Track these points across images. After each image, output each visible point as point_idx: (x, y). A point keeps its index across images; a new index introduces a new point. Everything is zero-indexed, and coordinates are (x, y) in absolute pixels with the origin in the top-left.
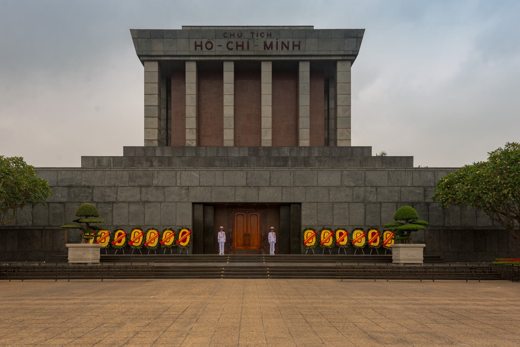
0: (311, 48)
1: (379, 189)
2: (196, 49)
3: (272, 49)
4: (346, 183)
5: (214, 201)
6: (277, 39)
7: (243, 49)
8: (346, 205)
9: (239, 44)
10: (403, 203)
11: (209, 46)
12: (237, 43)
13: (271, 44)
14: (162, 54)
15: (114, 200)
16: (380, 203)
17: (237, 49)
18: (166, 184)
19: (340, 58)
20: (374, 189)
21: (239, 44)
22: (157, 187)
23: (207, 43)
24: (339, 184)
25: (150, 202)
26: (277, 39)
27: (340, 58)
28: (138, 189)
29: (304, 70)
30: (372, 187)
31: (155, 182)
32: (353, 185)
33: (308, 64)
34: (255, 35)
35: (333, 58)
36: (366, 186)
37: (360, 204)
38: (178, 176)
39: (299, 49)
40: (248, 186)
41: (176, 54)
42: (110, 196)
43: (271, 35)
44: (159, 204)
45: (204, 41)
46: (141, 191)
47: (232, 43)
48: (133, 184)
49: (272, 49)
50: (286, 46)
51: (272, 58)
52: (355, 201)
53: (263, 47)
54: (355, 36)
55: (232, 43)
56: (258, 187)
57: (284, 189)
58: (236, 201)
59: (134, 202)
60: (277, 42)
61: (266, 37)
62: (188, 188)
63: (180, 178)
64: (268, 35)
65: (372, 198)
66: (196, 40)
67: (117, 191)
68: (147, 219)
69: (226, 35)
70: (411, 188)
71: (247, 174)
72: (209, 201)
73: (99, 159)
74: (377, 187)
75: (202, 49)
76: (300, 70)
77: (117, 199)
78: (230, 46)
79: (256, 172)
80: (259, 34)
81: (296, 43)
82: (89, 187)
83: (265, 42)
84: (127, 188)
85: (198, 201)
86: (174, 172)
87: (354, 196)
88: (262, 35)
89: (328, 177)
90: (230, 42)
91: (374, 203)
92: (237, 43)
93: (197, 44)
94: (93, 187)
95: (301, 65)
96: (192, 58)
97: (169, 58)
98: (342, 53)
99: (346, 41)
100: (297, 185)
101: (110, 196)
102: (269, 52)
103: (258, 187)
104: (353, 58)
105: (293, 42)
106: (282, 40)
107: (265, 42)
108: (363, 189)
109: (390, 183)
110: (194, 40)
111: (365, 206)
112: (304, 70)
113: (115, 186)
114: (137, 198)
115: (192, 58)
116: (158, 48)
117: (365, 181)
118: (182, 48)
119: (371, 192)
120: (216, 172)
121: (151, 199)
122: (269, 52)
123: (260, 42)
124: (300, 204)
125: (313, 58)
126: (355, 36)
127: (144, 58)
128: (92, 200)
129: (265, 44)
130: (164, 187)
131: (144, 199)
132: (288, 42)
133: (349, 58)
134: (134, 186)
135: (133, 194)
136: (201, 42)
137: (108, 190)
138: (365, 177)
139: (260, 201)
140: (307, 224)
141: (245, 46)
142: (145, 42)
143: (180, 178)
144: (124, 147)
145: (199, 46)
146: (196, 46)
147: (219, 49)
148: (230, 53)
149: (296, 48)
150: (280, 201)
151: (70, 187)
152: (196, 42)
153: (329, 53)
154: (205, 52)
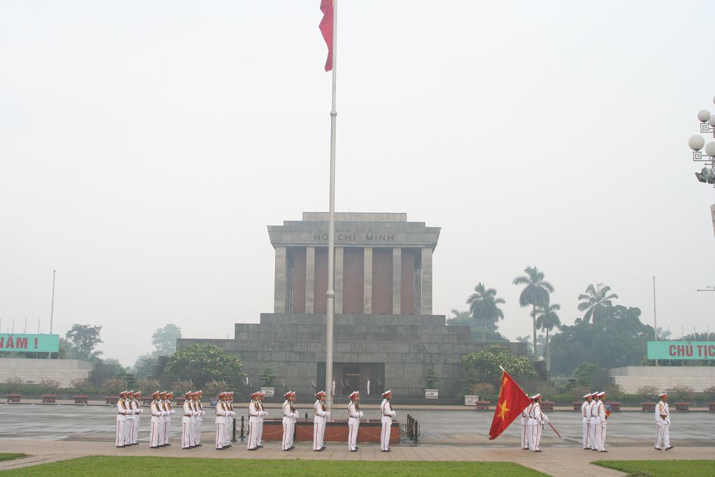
0: (402, 239)
4: (412, 351)
13: (372, 237)
22: (296, 352)
28: (284, 353)
30: (428, 353)
31: (295, 349)
33: (400, 250)
35: (418, 247)
54: (436, 232)
56: (358, 354)
65: (428, 361)
73: (248, 325)
74: (431, 353)
82: (255, 352)
98: (425, 243)
102: (370, 242)
110: (313, 234)
112: (397, 253)
116: (288, 239)
126: (436, 232)
137: (266, 354)
139: (359, 362)
142: (277, 234)
144: (261, 314)
146: (315, 237)
150: (371, 362)
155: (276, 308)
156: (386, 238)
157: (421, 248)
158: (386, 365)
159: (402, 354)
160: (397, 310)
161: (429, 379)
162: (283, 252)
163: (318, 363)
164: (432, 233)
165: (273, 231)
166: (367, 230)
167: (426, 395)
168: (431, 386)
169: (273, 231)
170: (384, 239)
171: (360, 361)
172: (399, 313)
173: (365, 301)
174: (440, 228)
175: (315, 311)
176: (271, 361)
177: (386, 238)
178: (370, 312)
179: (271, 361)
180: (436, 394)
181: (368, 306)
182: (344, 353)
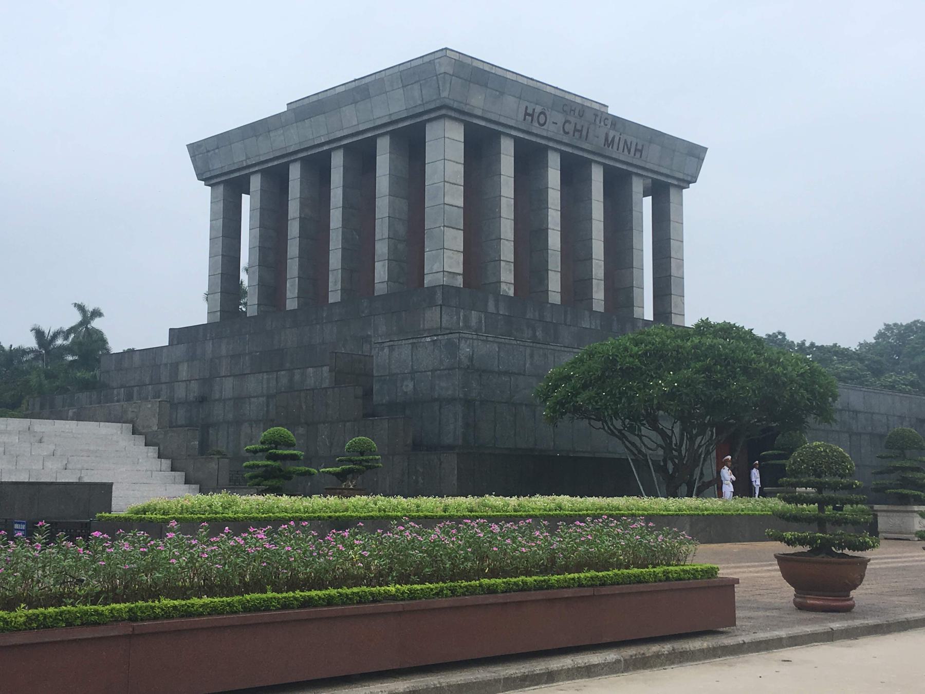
0: (653, 158)
7: (580, 137)
14: (479, 113)
21: (579, 127)
23: (541, 113)
27: (676, 183)
45: (538, 109)
51: (607, 162)
61: (609, 126)
69: (565, 108)
81: (639, 147)
83: (607, 135)
97: (483, 123)
98: (681, 176)
106: (623, 137)
107: (607, 135)
111: (850, 436)
116: (477, 101)
118: (509, 111)
122: (609, 151)
129: (606, 139)
141: (584, 133)
145: (529, 115)
146: (526, 114)
147: (552, 128)
149: (638, 155)
156: (633, 150)
170: (629, 151)
177: (633, 150)
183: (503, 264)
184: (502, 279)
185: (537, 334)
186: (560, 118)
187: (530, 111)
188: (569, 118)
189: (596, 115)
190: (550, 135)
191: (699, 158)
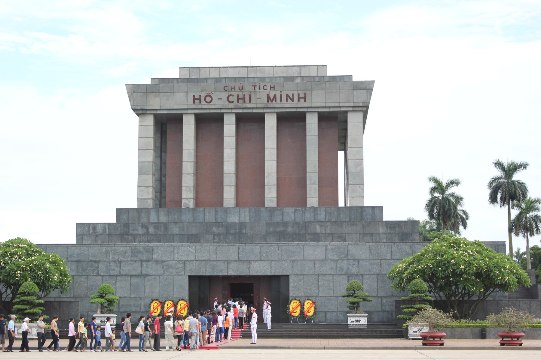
1: (361, 262)
2: (194, 103)
3: (276, 101)
4: (330, 256)
5: (208, 274)
6: (281, 92)
7: (244, 102)
8: (330, 278)
9: (240, 97)
10: (383, 274)
11: (208, 99)
12: (238, 96)
13: (275, 97)
14: (158, 107)
15: (118, 273)
16: (362, 275)
17: (238, 102)
18: (164, 259)
19: (351, 109)
20: (357, 263)
21: (240, 97)
22: (156, 261)
24: (324, 257)
25: (150, 275)
26: (281, 92)
27: (351, 109)
29: (312, 122)
30: (354, 260)
31: (155, 257)
32: (337, 259)
34: (257, 88)
35: (342, 109)
36: (348, 260)
37: (344, 276)
38: (175, 252)
39: (305, 101)
40: (239, 260)
41: (173, 108)
42: (114, 270)
43: (274, 87)
44: (158, 277)
45: (203, 95)
46: (142, 264)
47: (233, 96)
48: (135, 259)
49: (276, 101)
50: (290, 99)
52: (339, 273)
53: (266, 99)
54: (367, 87)
55: (233, 96)
56: (249, 262)
57: (273, 263)
58: (229, 274)
59: (135, 275)
60: (281, 95)
62: (184, 263)
63: (178, 253)
64: (271, 88)
65: (354, 270)
66: (194, 94)
67: (120, 265)
68: (147, 290)
69: (226, 88)
70: (391, 261)
71: (239, 249)
72: (204, 274)
74: (358, 261)
75: (200, 102)
76: (307, 122)
77: (120, 272)
78: (231, 99)
79: (247, 247)
80: (262, 87)
82: (95, 262)
84: (130, 262)
85: (193, 274)
86: (172, 248)
87: (338, 269)
88: (265, 88)
89: (313, 251)
90: (230, 95)
91: (357, 275)
92: (238, 96)
93: (196, 97)
94: (98, 262)
95: (308, 116)
96: (189, 111)
97: (165, 112)
98: (352, 105)
99: (355, 93)
100: (285, 259)
101: (114, 270)
102: (274, 104)
103: (249, 262)
104: (365, 109)
105: (299, 94)
106: (286, 92)
108: (345, 262)
109: (371, 256)
110: (192, 94)
111: (348, 277)
112: (312, 122)
113: (118, 261)
114: (138, 272)
115: (189, 111)
117: (347, 255)
119: (353, 265)
120: (211, 247)
121: (150, 272)
122: (274, 104)
123: (263, 95)
124: (288, 276)
125: (321, 110)
126: (367, 87)
127: (140, 112)
128: (98, 274)
129: (268, 97)
130: (163, 262)
131: (144, 272)
132: (293, 95)
133: (360, 109)
134: (136, 261)
135: (135, 268)
136: (200, 96)
137: (112, 264)
138: (348, 251)
140: (294, 295)
141: (247, 99)
142: (140, 96)
143: (178, 253)
146: (194, 99)
148: (231, 106)
149: (302, 100)
150: (269, 274)
151: (79, 261)
152: (194, 96)
153: (337, 105)
154: (204, 105)
155: (140, 200)
157: (346, 112)
158: (291, 279)
159: (314, 261)
160: (313, 200)
161: (352, 299)
162: (150, 121)
163: (190, 277)
164: (360, 89)
165: (135, 92)
166: (268, 88)
167: (349, 323)
168: (354, 307)
169: (135, 92)
171: (253, 272)
172: (316, 205)
173: (266, 187)
174: (374, 81)
175: (198, 203)
176: (120, 275)
178: (274, 204)
179: (120, 275)
180: (364, 321)
181: (271, 195)
182: (228, 262)
183: (183, 188)
184: (184, 196)
185: (150, 230)
186: (224, 95)
187: (197, 97)
188: (231, 93)
189: (255, 86)
190: (217, 106)
191: (367, 89)
